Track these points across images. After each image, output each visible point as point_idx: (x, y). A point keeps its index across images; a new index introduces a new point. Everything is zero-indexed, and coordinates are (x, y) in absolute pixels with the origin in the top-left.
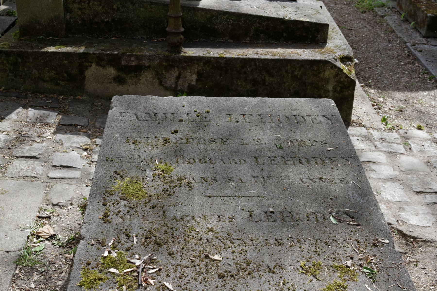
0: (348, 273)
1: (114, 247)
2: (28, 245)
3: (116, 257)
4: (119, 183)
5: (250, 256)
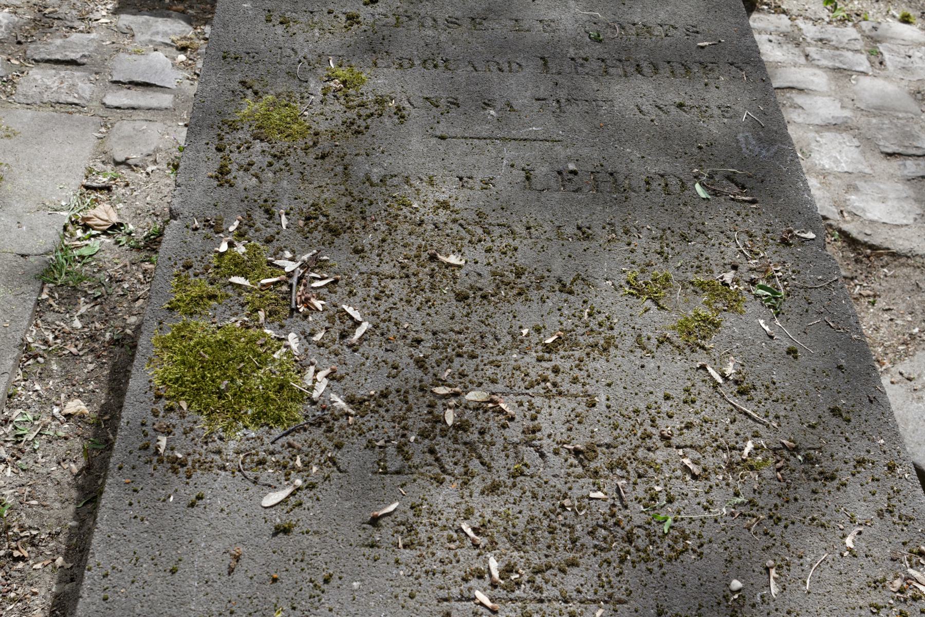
0: (725, 296)
1: (241, 235)
2: (66, 243)
3: (244, 254)
4: (249, 106)
5: (521, 259)
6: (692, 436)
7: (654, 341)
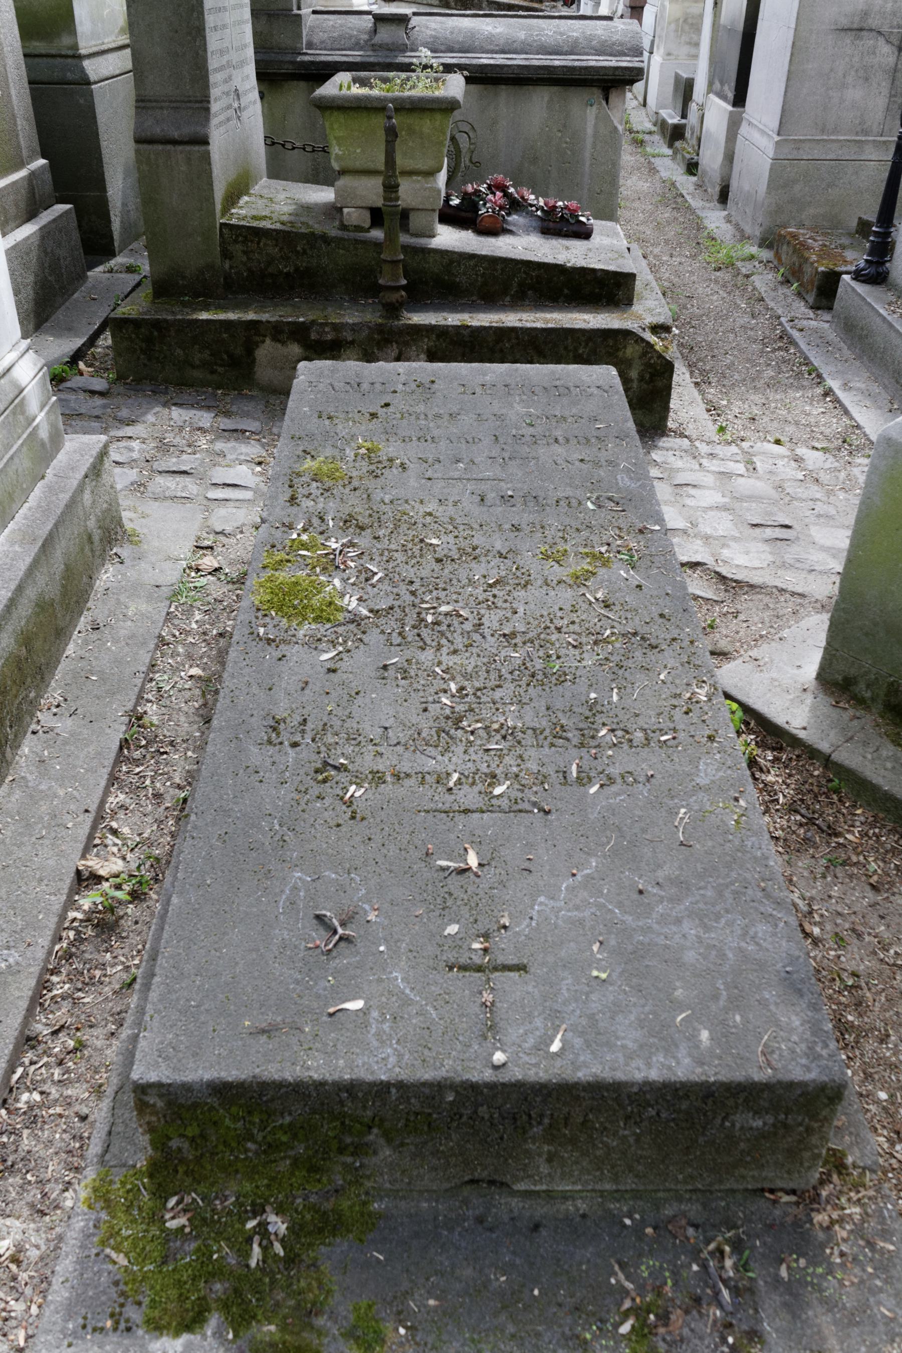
1: (305, 530)
4: (309, 463)
5: (475, 542)
6: (576, 628)
7: (555, 582)
